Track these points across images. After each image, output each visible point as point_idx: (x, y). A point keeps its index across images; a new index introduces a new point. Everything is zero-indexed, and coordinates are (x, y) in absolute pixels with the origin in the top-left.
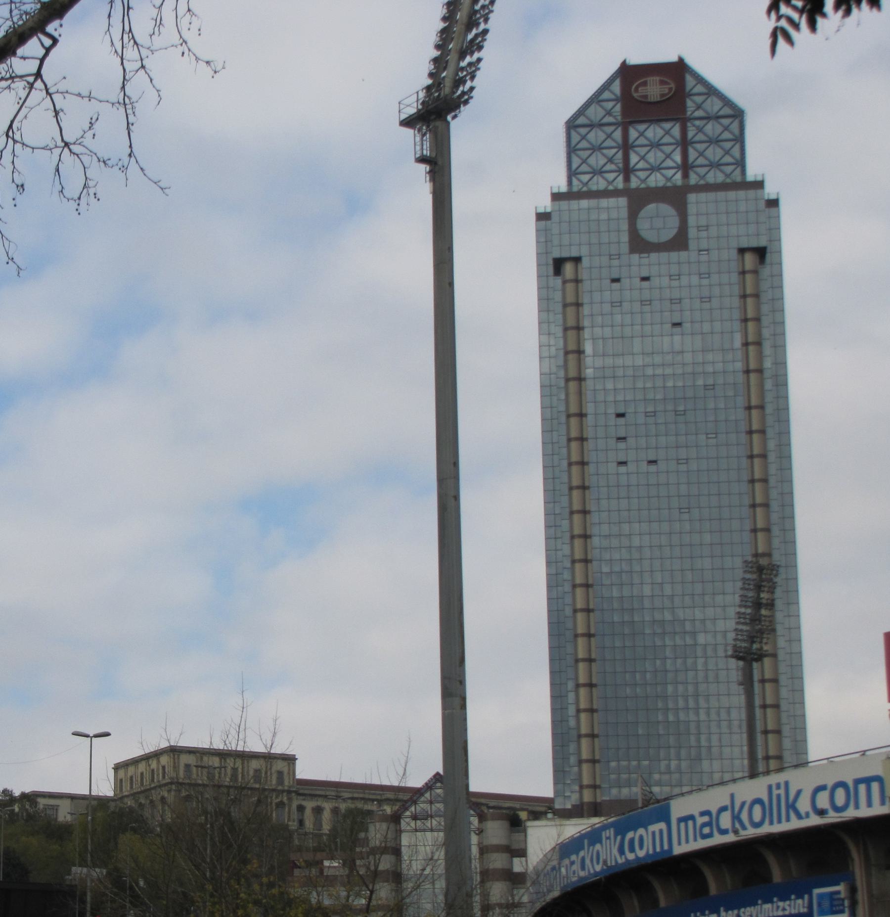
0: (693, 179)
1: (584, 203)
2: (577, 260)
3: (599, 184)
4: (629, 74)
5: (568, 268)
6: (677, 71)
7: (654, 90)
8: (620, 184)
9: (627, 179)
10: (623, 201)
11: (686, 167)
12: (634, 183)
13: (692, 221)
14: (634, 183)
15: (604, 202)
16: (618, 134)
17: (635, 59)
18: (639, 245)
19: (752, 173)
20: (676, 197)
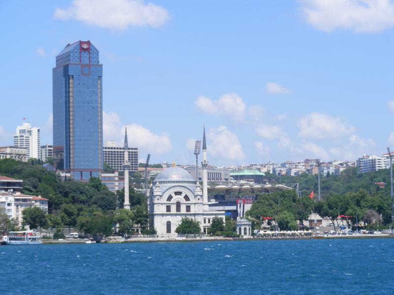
0: (91, 63)
1: (74, 66)
2: (73, 76)
3: (76, 63)
4: (81, 43)
5: (71, 77)
6: (88, 43)
7: (85, 46)
8: (79, 63)
9: (80, 62)
10: (80, 66)
11: (90, 61)
12: (82, 63)
13: (91, 71)
14: (82, 63)
15: (78, 66)
16: (78, 53)
17: (82, 40)
18: (83, 74)
19: (100, 63)
20: (89, 66)
